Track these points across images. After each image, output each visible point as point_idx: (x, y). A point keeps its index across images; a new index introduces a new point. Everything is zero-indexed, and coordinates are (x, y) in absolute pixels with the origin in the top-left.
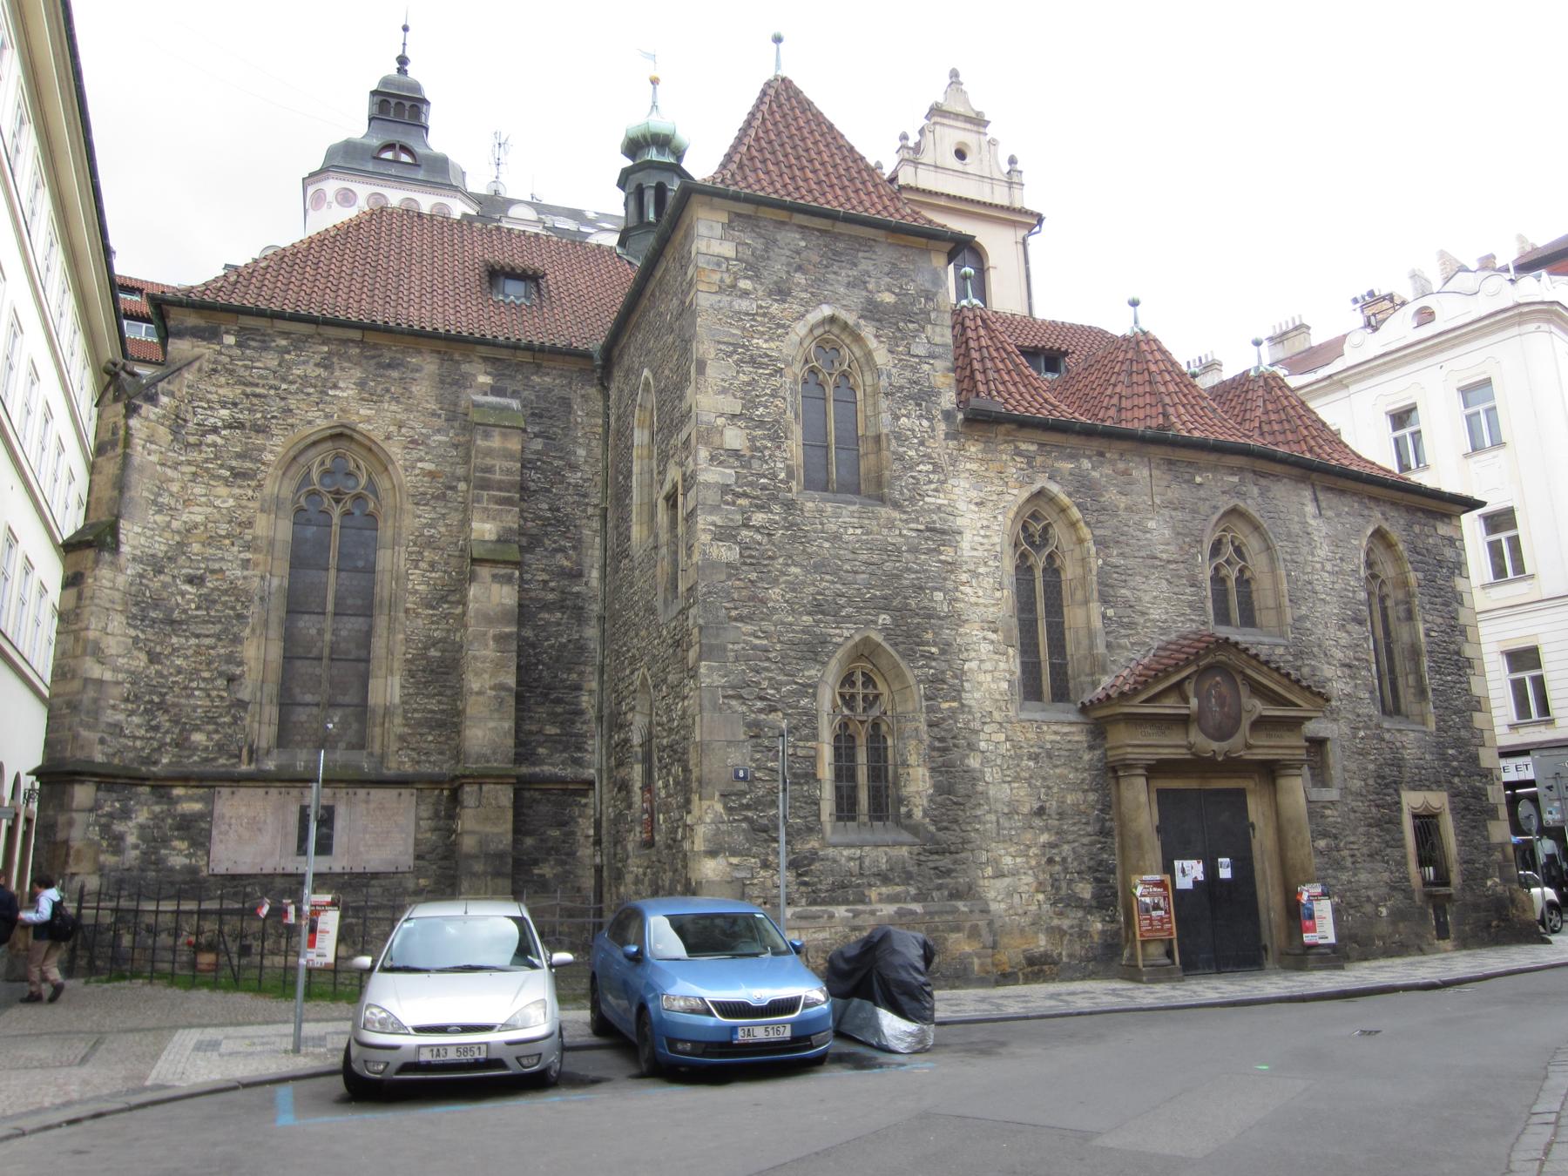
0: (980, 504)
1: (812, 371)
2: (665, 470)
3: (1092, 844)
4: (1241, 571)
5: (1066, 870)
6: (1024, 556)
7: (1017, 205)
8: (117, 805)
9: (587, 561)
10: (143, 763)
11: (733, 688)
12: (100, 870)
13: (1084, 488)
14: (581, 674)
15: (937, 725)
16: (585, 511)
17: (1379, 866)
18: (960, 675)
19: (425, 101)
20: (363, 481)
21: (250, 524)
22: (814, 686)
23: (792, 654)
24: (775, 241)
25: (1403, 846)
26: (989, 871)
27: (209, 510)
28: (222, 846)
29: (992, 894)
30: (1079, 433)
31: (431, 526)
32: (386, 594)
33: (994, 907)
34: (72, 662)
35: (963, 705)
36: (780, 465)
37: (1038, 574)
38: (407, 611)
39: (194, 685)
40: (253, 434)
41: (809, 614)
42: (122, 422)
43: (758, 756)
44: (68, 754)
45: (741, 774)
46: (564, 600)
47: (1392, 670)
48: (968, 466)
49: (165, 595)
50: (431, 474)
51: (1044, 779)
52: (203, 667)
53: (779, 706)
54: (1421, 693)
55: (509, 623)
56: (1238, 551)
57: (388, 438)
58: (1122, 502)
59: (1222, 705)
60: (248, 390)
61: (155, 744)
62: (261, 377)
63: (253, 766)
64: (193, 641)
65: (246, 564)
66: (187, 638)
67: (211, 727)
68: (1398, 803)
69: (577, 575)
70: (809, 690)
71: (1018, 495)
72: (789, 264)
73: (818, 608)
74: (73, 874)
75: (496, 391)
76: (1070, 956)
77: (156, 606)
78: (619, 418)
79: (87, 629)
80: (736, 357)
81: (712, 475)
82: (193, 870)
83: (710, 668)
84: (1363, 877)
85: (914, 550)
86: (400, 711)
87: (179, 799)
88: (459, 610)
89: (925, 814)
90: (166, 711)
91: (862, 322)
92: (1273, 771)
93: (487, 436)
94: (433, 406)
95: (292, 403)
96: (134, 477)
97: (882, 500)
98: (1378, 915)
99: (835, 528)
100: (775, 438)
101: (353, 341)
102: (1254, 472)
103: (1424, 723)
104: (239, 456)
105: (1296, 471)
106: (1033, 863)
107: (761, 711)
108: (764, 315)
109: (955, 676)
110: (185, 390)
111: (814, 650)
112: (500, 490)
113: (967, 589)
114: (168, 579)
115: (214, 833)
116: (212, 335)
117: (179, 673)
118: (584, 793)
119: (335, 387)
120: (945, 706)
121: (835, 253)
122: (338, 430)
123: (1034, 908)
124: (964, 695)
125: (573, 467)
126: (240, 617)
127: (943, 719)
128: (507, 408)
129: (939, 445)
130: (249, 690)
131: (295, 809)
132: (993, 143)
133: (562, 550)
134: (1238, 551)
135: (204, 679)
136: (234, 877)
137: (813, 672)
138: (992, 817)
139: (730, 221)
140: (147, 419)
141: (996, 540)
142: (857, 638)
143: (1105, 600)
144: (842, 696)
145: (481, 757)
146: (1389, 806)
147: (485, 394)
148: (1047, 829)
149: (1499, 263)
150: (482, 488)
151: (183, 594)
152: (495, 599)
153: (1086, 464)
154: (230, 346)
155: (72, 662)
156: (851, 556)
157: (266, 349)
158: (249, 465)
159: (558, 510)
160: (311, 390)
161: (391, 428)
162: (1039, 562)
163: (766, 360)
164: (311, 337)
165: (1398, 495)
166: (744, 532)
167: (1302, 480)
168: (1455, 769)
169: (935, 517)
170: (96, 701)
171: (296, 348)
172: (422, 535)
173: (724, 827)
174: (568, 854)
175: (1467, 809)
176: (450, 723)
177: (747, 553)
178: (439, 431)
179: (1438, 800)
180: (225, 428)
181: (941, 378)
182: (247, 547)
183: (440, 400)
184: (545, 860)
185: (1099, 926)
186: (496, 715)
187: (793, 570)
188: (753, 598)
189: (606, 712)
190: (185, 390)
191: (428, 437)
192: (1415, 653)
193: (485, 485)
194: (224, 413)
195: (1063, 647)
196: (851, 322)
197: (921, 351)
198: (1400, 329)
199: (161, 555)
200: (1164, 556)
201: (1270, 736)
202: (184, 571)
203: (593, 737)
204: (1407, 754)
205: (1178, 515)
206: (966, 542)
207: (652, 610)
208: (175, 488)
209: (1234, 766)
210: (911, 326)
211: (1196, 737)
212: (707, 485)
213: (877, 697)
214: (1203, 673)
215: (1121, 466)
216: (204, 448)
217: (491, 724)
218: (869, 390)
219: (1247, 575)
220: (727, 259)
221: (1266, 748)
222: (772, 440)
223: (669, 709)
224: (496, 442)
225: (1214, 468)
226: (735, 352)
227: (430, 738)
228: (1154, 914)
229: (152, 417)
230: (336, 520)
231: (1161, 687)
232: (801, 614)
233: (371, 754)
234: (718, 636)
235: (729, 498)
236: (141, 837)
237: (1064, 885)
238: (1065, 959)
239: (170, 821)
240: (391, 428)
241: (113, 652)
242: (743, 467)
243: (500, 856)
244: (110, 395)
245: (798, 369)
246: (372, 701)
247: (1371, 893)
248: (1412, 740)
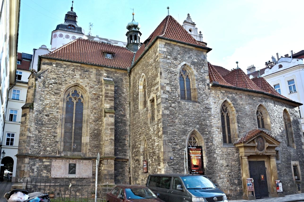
0: (215, 103)
1: (181, 75)
2: (150, 95)
3: (237, 172)
4: (262, 117)
5: (232, 178)
6: (222, 114)
7: (202, 41)
8: (33, 163)
9: (126, 113)
10: (38, 154)
11: (169, 140)
12: (30, 176)
13: (233, 100)
14: (125, 137)
15: (208, 148)
16: (126, 102)
17: (288, 176)
18: (212, 138)
19: (76, 16)
20: (80, 95)
21: (58, 104)
22: (185, 140)
23: (180, 133)
24: (174, 48)
25: (292, 172)
26: (218, 178)
27: (50, 101)
28: (53, 172)
29: (219, 183)
30: (233, 89)
31: (95, 105)
32: (86, 119)
33: (220, 185)
34: (24, 132)
35: (213, 144)
36: (177, 94)
37: (225, 117)
38: (90, 123)
39: (47, 138)
40: (59, 85)
41: (183, 125)
42: (34, 82)
43: (174, 154)
44: (24, 152)
45: (171, 158)
46: (122, 121)
47: (288, 137)
48: (212, 95)
49: (41, 118)
50: (95, 94)
51: (228, 159)
52: (49, 134)
53: (178, 144)
54: (293, 142)
55: (113, 126)
56: (261, 113)
57: (86, 86)
58: (241, 103)
59: (261, 144)
60: (58, 76)
61: (40, 150)
62: (60, 73)
63: (59, 155)
64: (47, 128)
65: (57, 112)
66: (46, 128)
67: (51, 147)
68: (291, 163)
69: (124, 116)
70: (184, 141)
71: (222, 101)
72: (177, 53)
73: (185, 124)
74: (25, 177)
75: (108, 77)
76: (233, 195)
77: (40, 121)
78: (134, 83)
79: (27, 125)
80: (167, 72)
82: (47, 177)
83: (165, 136)
84: (285, 178)
85: (203, 112)
86: (89, 144)
87: (45, 162)
88: (100, 123)
89: (206, 166)
90: (42, 143)
91: (191, 65)
92: (269, 157)
93: (107, 86)
94: (95, 80)
95: (67, 78)
96: (36, 94)
97: (196, 102)
98: (288, 185)
99: (188, 107)
100: (176, 88)
101: (79, 66)
102: (264, 97)
103: (294, 148)
104: (56, 90)
105: (271, 97)
106: (227, 176)
107: (175, 145)
108: (173, 63)
109: (211, 138)
110: (46, 76)
111: (184, 132)
112: (110, 98)
113: (213, 120)
114: (42, 115)
115: (52, 169)
116: (51, 64)
117: (44, 135)
118: (126, 162)
119: (75, 75)
120: (210, 144)
121: (186, 51)
122: (76, 84)
123: (227, 185)
124: (213, 142)
125: (123, 93)
126: (56, 123)
127: (209, 147)
128: (110, 81)
129: (207, 91)
130: (58, 139)
131: (68, 164)
132: (196, 28)
133: (121, 110)
134: (261, 113)
135: (49, 136)
136: (56, 178)
137: (184, 137)
138: (219, 167)
139: (165, 44)
140: (39, 82)
141: (218, 110)
142: (193, 130)
143: (238, 123)
144: (189, 142)
145: (108, 154)
146: (289, 164)
147: (105, 77)
148: (229, 169)
149: (289, 56)
150: (107, 97)
151: (45, 118)
152: (110, 120)
153: (234, 95)
154: (54, 67)
155: (24, 132)
156: (191, 113)
157: (61, 67)
158: (58, 92)
159: (120, 102)
160: (70, 76)
161: (87, 84)
162: (225, 115)
163: (173, 72)
164: (70, 65)
165: (288, 102)
166: (170, 108)
167: (272, 99)
168: (299, 157)
169: (207, 105)
170: (29, 141)
171: (67, 67)
172: (93, 107)
173: (168, 169)
174: (124, 174)
175: (302, 165)
176: (98, 147)
177: (171, 112)
178: (96, 85)
179: (297, 163)
180: (53, 84)
181: (206, 76)
182: (58, 109)
183: (96, 78)
184: (119, 176)
185: (239, 189)
186: (110, 145)
187: (180, 116)
188: (172, 122)
189: (131, 145)
190: (46, 76)
191: (94, 86)
192: (292, 133)
194: (53, 80)
195: (230, 132)
196: (189, 65)
197: (202, 71)
198: (276, 68)
199: (41, 110)
200: (249, 114)
201: (269, 150)
202: (45, 114)
203: (128, 150)
204: (292, 154)
205: (251, 106)
206: (213, 110)
207: (146, 123)
208: (43, 96)
209: (263, 156)
210: (200, 66)
211: (256, 150)
212: (163, 98)
213: (196, 142)
214: (257, 137)
215: (240, 96)
216: (49, 88)
217: (110, 147)
218: (193, 79)
219: (263, 118)
220: (165, 52)
221: (269, 152)
222: (175, 89)
223: (152, 144)
224: (109, 88)
225: (257, 97)
226: (167, 71)
227: (95, 150)
228: (250, 186)
229: (40, 81)
230: (75, 103)
231: (250, 140)
232: (182, 125)
233: (83, 153)
234: (166, 129)
235: (167, 101)
236: (37, 170)
237: (232, 181)
238: (233, 196)
239: (43, 166)
240: (87, 84)
241: (32, 130)
242: (170, 94)
243: (112, 175)
244: (31, 76)
245: (178, 76)
246: (83, 141)
247: (287, 182)
248: (292, 151)
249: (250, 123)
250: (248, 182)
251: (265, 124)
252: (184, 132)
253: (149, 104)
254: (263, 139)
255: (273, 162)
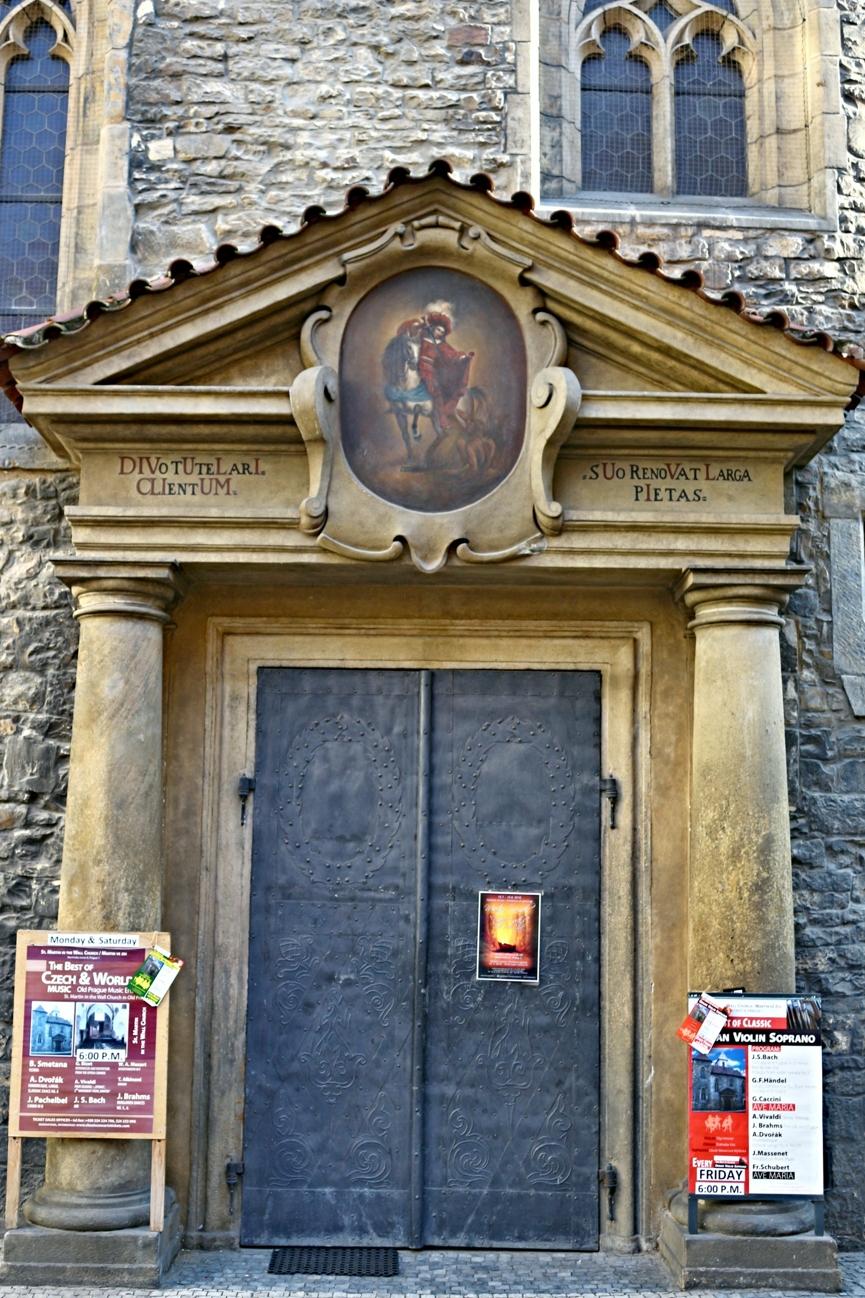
59: (447, 393)
143: (143, 115)
219: (730, 39)
221: (623, 528)
228: (84, 1057)
249: (367, 107)
250: (58, 984)
251: (753, 128)
254: (510, 315)
255: (738, 677)
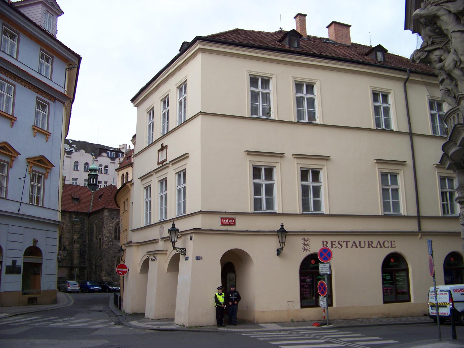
69: (85, 241)
70: (114, 261)
73: (115, 253)
75: (76, 218)
81: (105, 239)
111: (114, 257)
128: (77, 221)
193: (76, 232)
224: (77, 226)
252: (114, 257)
253: (98, 240)
